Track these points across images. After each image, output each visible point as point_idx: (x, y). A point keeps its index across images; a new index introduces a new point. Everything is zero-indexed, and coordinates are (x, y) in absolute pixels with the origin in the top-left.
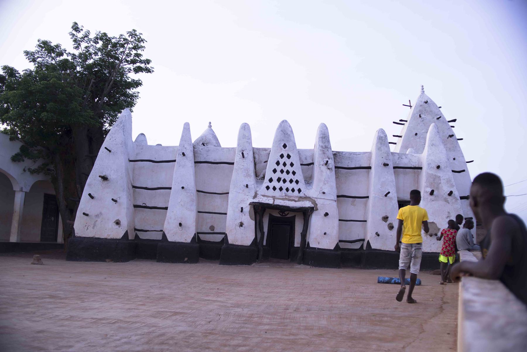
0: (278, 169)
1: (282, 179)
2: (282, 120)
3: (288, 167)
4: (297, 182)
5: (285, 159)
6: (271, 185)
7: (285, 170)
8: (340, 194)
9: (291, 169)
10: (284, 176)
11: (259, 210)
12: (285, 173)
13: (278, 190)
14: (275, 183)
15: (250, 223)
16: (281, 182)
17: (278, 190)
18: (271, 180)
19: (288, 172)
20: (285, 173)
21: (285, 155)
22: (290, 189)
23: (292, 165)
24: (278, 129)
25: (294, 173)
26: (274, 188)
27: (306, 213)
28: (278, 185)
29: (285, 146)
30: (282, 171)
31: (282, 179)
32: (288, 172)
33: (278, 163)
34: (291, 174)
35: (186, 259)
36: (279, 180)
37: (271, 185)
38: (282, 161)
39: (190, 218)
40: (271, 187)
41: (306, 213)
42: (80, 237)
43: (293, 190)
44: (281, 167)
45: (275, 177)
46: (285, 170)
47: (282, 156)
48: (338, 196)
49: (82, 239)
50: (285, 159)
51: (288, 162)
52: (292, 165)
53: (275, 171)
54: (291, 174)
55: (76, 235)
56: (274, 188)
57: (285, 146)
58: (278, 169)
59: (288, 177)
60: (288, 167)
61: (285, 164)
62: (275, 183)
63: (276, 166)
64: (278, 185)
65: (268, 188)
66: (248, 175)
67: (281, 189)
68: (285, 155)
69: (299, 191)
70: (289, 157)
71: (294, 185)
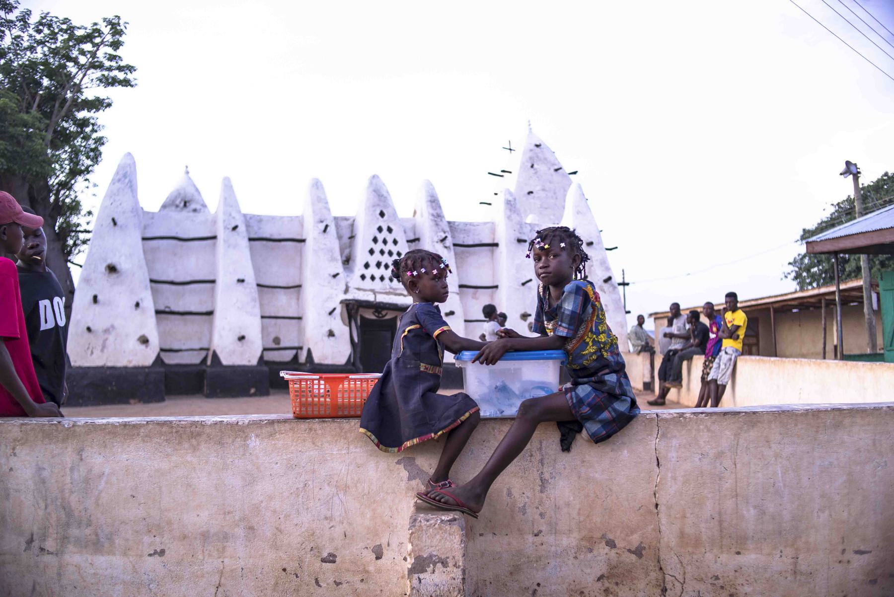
1: (383, 264)
2: (373, 174)
3: (390, 246)
11: (352, 309)
12: (386, 255)
13: (377, 280)
14: (373, 270)
15: (342, 330)
16: (382, 267)
17: (377, 280)
20: (386, 255)
21: (385, 228)
23: (395, 242)
24: (368, 188)
26: (373, 278)
29: (382, 214)
30: (382, 252)
31: (383, 264)
33: (375, 240)
35: (253, 391)
39: (253, 328)
40: (368, 277)
42: (80, 368)
45: (373, 260)
47: (380, 229)
48: (461, 286)
49: (85, 372)
52: (395, 242)
53: (372, 252)
55: (72, 364)
56: (373, 278)
57: (382, 214)
61: (385, 242)
63: (372, 245)
65: (363, 277)
66: (333, 259)
68: (385, 228)
70: (390, 230)
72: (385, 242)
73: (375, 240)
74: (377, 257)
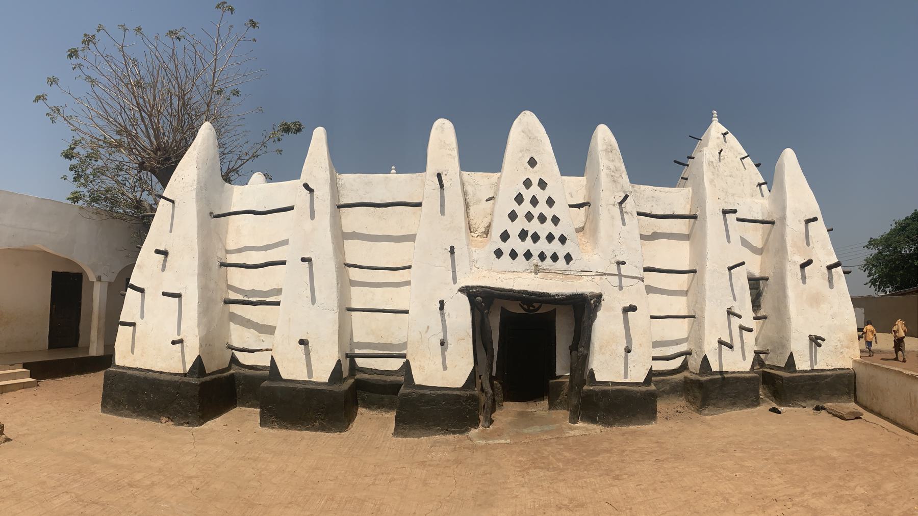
0: (521, 210)
3: (542, 208)
4: (563, 240)
5: (535, 190)
6: (506, 247)
7: (536, 212)
8: (692, 220)
9: (549, 213)
10: (534, 226)
12: (535, 221)
14: (514, 243)
17: (521, 257)
18: (505, 236)
19: (542, 219)
20: (535, 221)
21: (535, 182)
22: (549, 255)
23: (550, 202)
26: (514, 255)
27: (583, 308)
28: (521, 247)
29: (532, 163)
30: (529, 217)
31: (530, 234)
32: (542, 219)
33: (519, 199)
34: (549, 222)
36: (523, 235)
37: (506, 247)
38: (527, 195)
41: (583, 308)
43: (555, 258)
44: (527, 206)
45: (514, 229)
46: (536, 212)
47: (528, 183)
50: (535, 190)
51: (542, 196)
52: (550, 202)
53: (513, 216)
54: (549, 222)
56: (514, 255)
57: (532, 163)
58: (521, 210)
60: (542, 208)
61: (534, 201)
62: (514, 243)
63: (515, 206)
64: (521, 247)
65: (499, 253)
67: (528, 255)
69: (568, 258)
70: (542, 184)
71: (556, 246)
72: (534, 201)
73: (519, 199)
74: (522, 223)
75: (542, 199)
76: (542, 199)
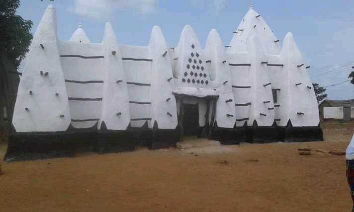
3: (198, 64)
5: (195, 57)
8: (249, 106)
9: (200, 66)
10: (195, 71)
14: (189, 77)
21: (195, 54)
23: (200, 62)
25: (202, 68)
26: (189, 81)
28: (191, 78)
29: (193, 47)
30: (194, 67)
32: (198, 68)
33: (190, 61)
34: (200, 69)
37: (186, 78)
41: (211, 101)
44: (192, 64)
45: (189, 71)
47: (192, 55)
50: (195, 57)
51: (198, 60)
52: (200, 62)
59: (199, 72)
61: (195, 62)
64: (191, 78)
70: (197, 55)
71: (202, 78)
72: (195, 62)
75: (198, 61)
76: (198, 61)
